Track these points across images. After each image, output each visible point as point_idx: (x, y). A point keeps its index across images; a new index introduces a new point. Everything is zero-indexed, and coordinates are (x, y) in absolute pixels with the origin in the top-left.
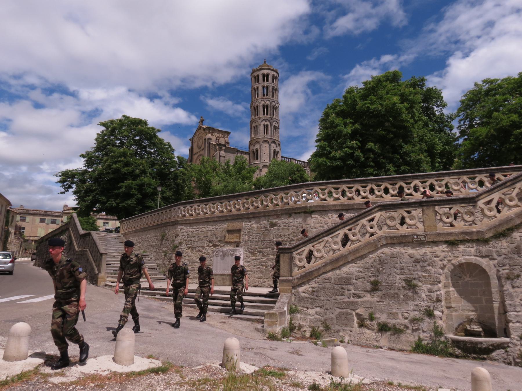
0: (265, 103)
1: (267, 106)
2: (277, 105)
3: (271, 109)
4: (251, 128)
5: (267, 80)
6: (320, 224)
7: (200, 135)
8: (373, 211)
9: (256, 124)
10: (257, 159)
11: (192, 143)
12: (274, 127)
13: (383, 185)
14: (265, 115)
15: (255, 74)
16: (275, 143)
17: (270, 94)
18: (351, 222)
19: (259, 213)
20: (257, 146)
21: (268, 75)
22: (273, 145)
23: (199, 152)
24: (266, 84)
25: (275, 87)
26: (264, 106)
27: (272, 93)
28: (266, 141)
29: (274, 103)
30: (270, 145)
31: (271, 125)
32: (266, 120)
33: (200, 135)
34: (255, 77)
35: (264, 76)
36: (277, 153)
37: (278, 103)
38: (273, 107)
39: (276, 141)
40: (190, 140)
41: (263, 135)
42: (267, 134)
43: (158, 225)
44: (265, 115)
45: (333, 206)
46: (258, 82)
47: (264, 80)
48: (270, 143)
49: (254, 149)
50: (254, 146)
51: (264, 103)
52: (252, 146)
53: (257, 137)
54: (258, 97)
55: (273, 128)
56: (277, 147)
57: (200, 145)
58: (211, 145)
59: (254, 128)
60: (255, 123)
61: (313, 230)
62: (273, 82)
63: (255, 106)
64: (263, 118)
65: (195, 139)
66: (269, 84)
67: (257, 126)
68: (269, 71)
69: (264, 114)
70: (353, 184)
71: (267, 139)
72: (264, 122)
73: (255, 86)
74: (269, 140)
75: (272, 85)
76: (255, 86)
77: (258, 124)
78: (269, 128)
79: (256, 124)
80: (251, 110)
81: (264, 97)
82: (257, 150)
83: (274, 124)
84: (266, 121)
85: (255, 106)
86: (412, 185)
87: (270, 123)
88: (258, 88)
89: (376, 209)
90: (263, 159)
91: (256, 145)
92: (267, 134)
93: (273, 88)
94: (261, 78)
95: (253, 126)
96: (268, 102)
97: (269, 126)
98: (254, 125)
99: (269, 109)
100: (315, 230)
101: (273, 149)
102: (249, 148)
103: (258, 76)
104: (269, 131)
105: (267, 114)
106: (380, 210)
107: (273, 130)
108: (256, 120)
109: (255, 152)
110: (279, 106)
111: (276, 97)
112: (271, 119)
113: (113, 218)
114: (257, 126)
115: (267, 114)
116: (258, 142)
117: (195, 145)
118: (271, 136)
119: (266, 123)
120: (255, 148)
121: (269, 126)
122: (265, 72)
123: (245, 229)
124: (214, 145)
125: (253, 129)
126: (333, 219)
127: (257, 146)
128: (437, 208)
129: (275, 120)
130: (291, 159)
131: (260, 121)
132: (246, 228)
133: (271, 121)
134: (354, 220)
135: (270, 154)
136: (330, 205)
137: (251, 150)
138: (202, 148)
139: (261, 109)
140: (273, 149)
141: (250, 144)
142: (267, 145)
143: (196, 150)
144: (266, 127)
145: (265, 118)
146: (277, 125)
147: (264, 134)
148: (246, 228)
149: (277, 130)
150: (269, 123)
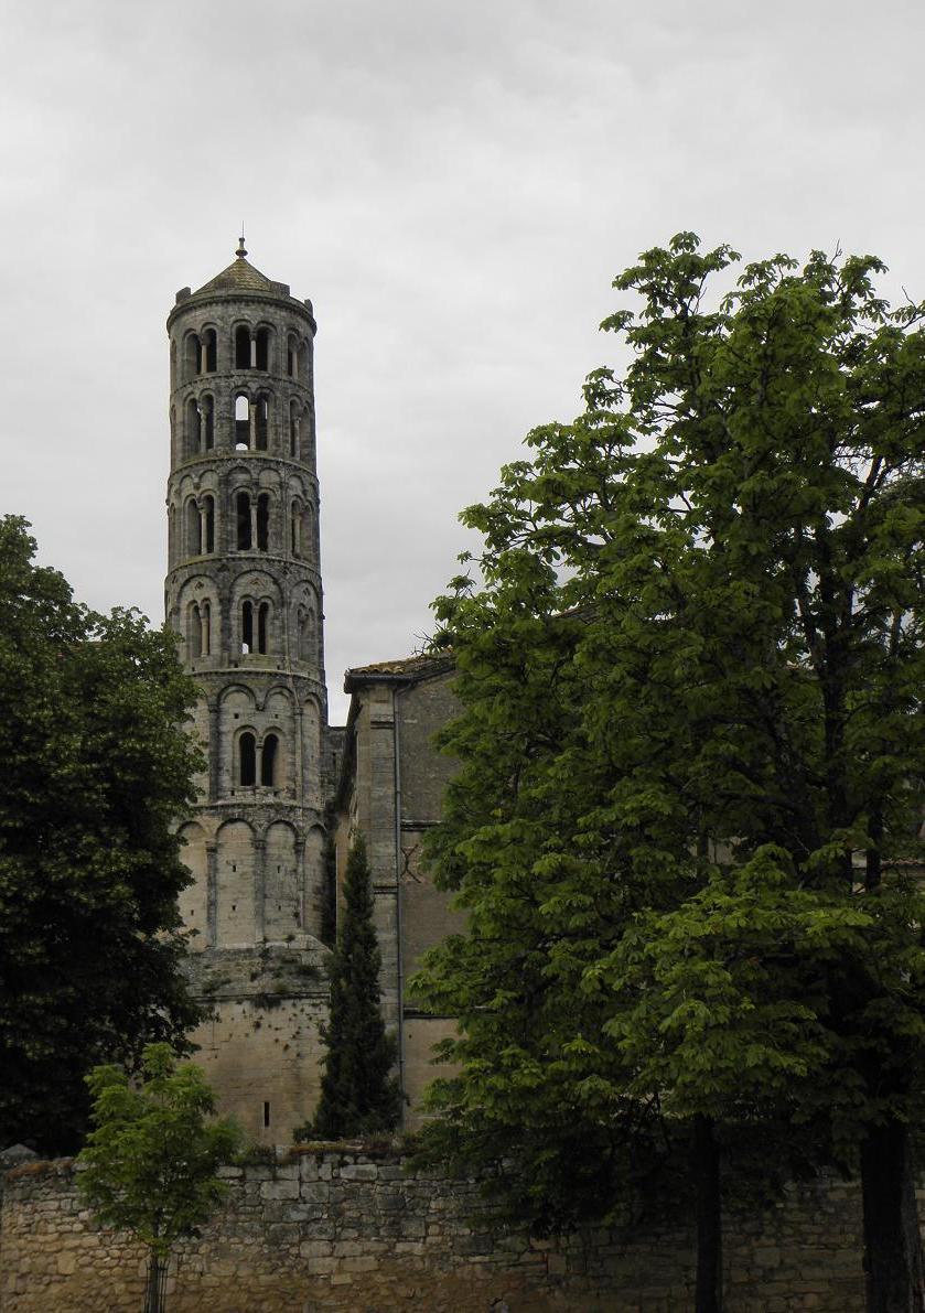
14: (204, 555)
44: (204, 555)
66: (213, 386)
84: (201, 585)
97: (216, 608)
105: (210, 550)
115: (210, 550)
119: (199, 595)
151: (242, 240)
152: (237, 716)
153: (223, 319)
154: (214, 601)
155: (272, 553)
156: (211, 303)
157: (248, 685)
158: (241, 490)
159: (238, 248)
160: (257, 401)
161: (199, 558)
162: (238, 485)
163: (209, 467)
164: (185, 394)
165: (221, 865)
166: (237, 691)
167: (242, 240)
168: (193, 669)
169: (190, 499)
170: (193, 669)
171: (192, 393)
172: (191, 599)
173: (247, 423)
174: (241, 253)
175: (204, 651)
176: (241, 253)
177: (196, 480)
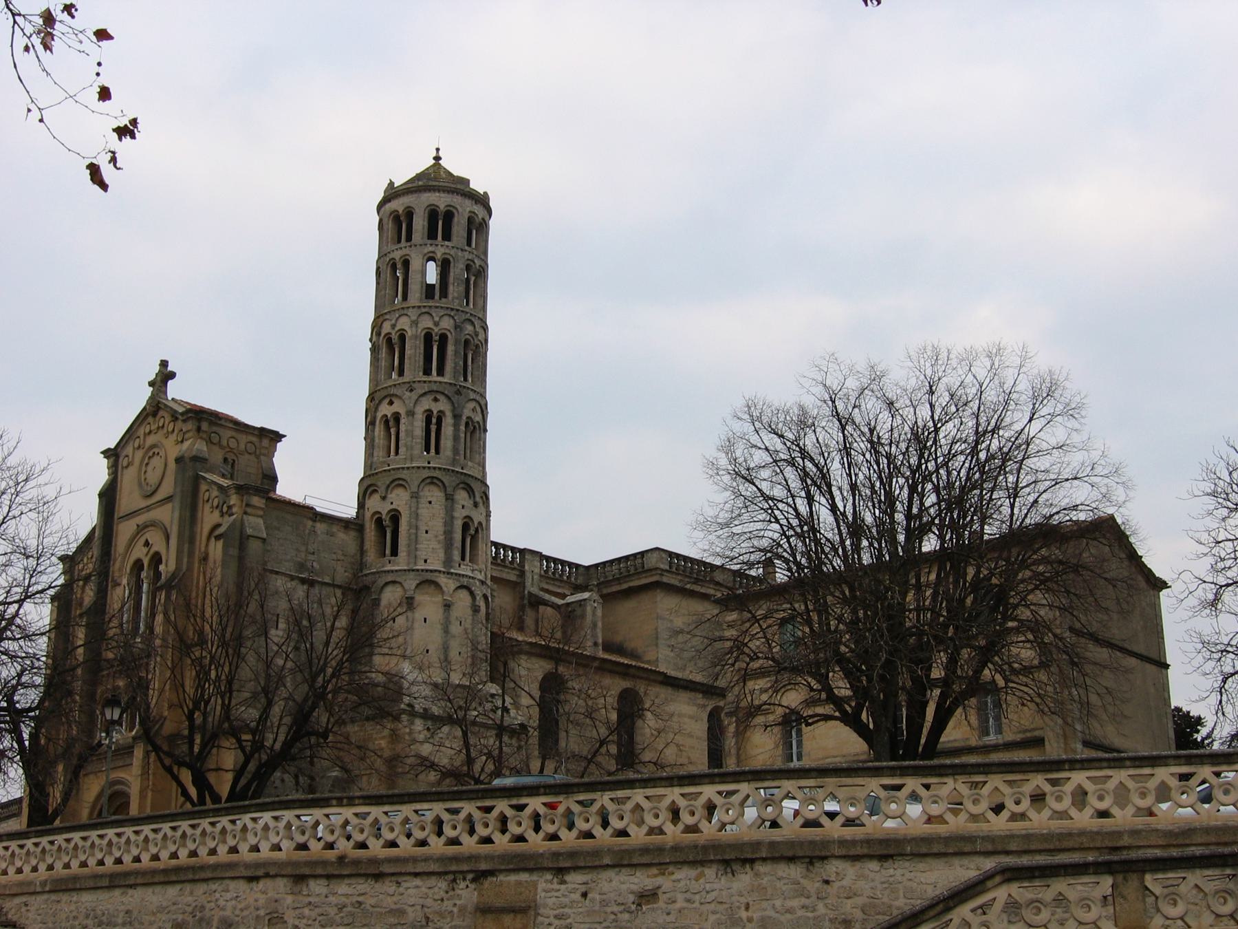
0: (436, 324)
1: (443, 339)
2: (481, 337)
3: (456, 352)
4: (370, 424)
5: (447, 236)
6: (804, 901)
7: (151, 440)
8: (989, 884)
9: (398, 407)
10: (395, 552)
11: (114, 470)
12: (467, 424)
13: (987, 785)
14: (434, 376)
15: (398, 205)
16: (470, 490)
17: (454, 290)
18: (932, 913)
19: (596, 853)
20: (399, 499)
21: (449, 216)
22: (462, 496)
23: (148, 508)
25: (478, 262)
26: (428, 338)
27: (462, 288)
28: (432, 481)
29: (469, 328)
30: (449, 498)
31: (457, 417)
32: (435, 394)
33: (151, 440)
34: (396, 218)
35: (433, 214)
36: (477, 531)
38: (467, 342)
40: (107, 453)
41: (421, 456)
42: (437, 452)
43: (177, 870)
44: (434, 376)
45: (842, 843)
46: (409, 238)
47: (432, 235)
48: (449, 490)
49: (384, 513)
50: (384, 498)
51: (430, 325)
52: (376, 497)
53: (396, 462)
54: (405, 298)
55: (463, 428)
56: (476, 505)
57: (153, 477)
58: (203, 487)
59: (387, 422)
60: (391, 403)
61: (782, 918)
62: (469, 244)
63: (395, 338)
64: (426, 388)
65: (129, 450)
66: (452, 252)
67: (397, 417)
68: (456, 200)
69: (427, 372)
70: (902, 775)
71: (437, 474)
72: (427, 403)
73: (397, 255)
74: (446, 479)
75: (467, 256)
76: (397, 255)
77: (402, 411)
78: (448, 429)
79: (398, 407)
80: (375, 350)
81: (431, 303)
82: (395, 517)
83: (467, 412)
84: (436, 400)
85: (395, 338)
86: (1069, 788)
87: (454, 409)
89: (998, 879)
90: (422, 555)
91: (392, 496)
92: (437, 452)
93: (468, 268)
94: (420, 223)
95: (379, 415)
96: (447, 324)
98: (385, 410)
99: (450, 349)
100: (788, 916)
101: (459, 514)
102: (361, 505)
103: (409, 214)
104: (447, 443)
106: (1008, 880)
107: (462, 435)
108: (393, 391)
109: (387, 522)
111: (480, 303)
112: (458, 393)
113: (166, 879)
114: (397, 417)
115: (441, 372)
116: (398, 483)
117: (128, 479)
118: (454, 462)
119: (436, 408)
120: (384, 508)
121: (448, 421)
122: (441, 201)
123: (545, 906)
124: (220, 487)
125: (379, 430)
126: (844, 883)
127: (399, 499)
128: (1148, 878)
129: (472, 396)
130: (523, 551)
131: (414, 396)
132: (550, 902)
133: (455, 398)
134: (941, 907)
135: (448, 533)
136: (834, 842)
137: (368, 515)
138: (159, 496)
139: (414, 350)
140: (459, 514)
141: (367, 489)
142: (435, 495)
143: (128, 499)
144: (433, 422)
145: (435, 387)
146: (478, 418)
147: (428, 450)
148: (550, 902)
150: (443, 405)
151: (438, 150)
152: (463, 507)
153: (420, 203)
154: (449, 414)
155: (407, 377)
156: (453, 192)
158: (468, 337)
159: (434, 154)
160: (444, 267)
161: (430, 378)
163: (448, 312)
164: (426, 251)
165: (453, 619)
166: (463, 488)
167: (438, 150)
171: (433, 252)
172: (427, 408)
173: (433, 286)
174: (437, 158)
175: (433, 450)
176: (437, 158)
177: (437, 319)
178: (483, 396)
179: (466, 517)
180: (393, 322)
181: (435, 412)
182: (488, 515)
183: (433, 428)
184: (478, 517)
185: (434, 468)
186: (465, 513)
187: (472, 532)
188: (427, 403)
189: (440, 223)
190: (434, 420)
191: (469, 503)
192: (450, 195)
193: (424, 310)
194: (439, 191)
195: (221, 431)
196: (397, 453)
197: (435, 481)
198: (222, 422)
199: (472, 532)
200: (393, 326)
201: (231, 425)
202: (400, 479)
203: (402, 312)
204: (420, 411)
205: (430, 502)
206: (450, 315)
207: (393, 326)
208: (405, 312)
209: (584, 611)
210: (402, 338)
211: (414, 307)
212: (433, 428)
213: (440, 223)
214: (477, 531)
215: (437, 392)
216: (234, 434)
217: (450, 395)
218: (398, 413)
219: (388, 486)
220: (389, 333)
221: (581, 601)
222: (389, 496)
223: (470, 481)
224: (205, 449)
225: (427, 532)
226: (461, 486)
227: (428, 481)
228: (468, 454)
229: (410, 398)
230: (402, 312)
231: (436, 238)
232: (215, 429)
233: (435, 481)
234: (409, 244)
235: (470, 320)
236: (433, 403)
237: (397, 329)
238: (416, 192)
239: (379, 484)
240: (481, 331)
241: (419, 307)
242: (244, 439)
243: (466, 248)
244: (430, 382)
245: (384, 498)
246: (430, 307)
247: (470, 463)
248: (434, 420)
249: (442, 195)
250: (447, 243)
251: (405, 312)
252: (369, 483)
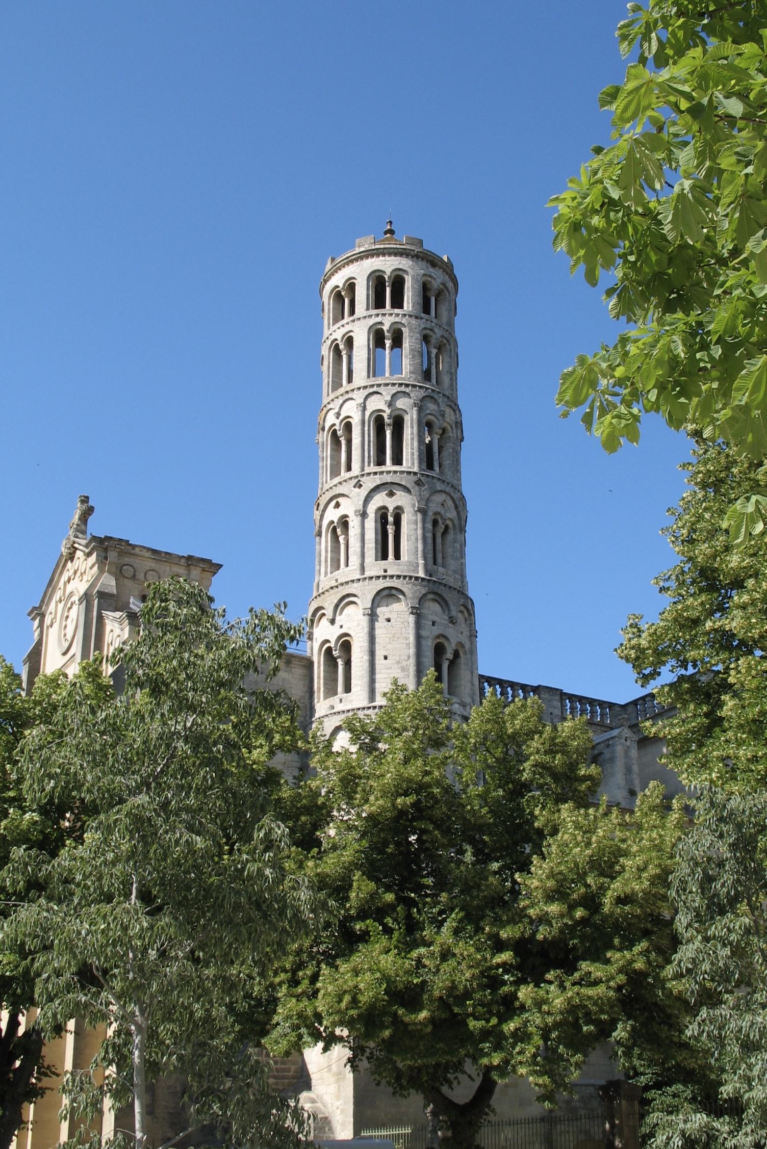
2: (450, 415)
5: (398, 302)
14: (389, 466)
21: (398, 283)
24: (388, 319)
32: (389, 488)
36: (456, 654)
37: (455, 408)
39: (447, 595)
44: (389, 466)
46: (352, 312)
47: (379, 303)
50: (332, 622)
54: (350, 380)
56: (452, 620)
60: (337, 505)
64: (378, 480)
66: (404, 321)
72: (380, 500)
84: (391, 494)
88: (349, 342)
94: (362, 294)
103: (351, 287)
110: (459, 424)
115: (397, 460)
119: (391, 504)
131: (364, 492)
145: (388, 478)
147: (385, 557)
149: (451, 536)
152: (434, 623)
157: (445, 596)
158: (430, 417)
161: (383, 468)
162: (428, 412)
166: (434, 600)
168: (385, 571)
169: (376, 414)
170: (385, 571)
171: (381, 323)
172: (381, 504)
178: (457, 488)
179: (438, 637)
180: (337, 410)
181: (391, 509)
182: (473, 635)
183: (391, 529)
184: (455, 636)
185: (392, 577)
186: (436, 631)
187: (449, 655)
188: (380, 500)
189: (388, 290)
190: (391, 519)
191: (442, 619)
192: (398, 258)
193: (372, 390)
194: (384, 255)
195: (136, 562)
196: (347, 565)
197: (394, 592)
198: (137, 550)
199: (449, 655)
200: (338, 415)
201: (148, 554)
202: (348, 595)
203: (346, 397)
204: (372, 509)
205: (389, 620)
206: (404, 392)
207: (338, 415)
208: (350, 395)
209: (613, 752)
210: (348, 427)
211: (359, 389)
212: (391, 529)
213: (388, 290)
214: (456, 654)
215: (392, 483)
216: (153, 565)
217: (408, 485)
218: (346, 516)
219: (337, 606)
220: (334, 425)
221: (608, 740)
222: (338, 618)
223: (441, 590)
224: (113, 583)
225: (386, 658)
226: (431, 596)
227: (386, 592)
228: (439, 560)
229: (358, 495)
230: (346, 397)
231: (384, 307)
232: (127, 560)
233: (394, 592)
234: (352, 318)
235: (432, 397)
236: (387, 498)
237: (341, 418)
238: (357, 260)
239: (325, 605)
240: (448, 411)
241: (365, 387)
242: (165, 568)
243: (423, 315)
244: (382, 473)
245: (332, 622)
246: (379, 385)
247: (441, 569)
248: (391, 519)
249: (387, 258)
250: (397, 311)
251: (350, 395)
252: (316, 606)
